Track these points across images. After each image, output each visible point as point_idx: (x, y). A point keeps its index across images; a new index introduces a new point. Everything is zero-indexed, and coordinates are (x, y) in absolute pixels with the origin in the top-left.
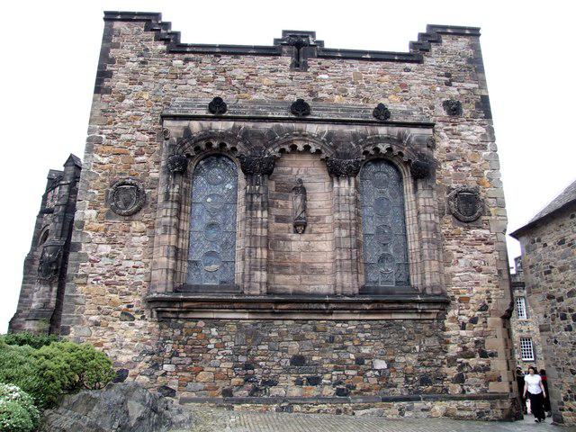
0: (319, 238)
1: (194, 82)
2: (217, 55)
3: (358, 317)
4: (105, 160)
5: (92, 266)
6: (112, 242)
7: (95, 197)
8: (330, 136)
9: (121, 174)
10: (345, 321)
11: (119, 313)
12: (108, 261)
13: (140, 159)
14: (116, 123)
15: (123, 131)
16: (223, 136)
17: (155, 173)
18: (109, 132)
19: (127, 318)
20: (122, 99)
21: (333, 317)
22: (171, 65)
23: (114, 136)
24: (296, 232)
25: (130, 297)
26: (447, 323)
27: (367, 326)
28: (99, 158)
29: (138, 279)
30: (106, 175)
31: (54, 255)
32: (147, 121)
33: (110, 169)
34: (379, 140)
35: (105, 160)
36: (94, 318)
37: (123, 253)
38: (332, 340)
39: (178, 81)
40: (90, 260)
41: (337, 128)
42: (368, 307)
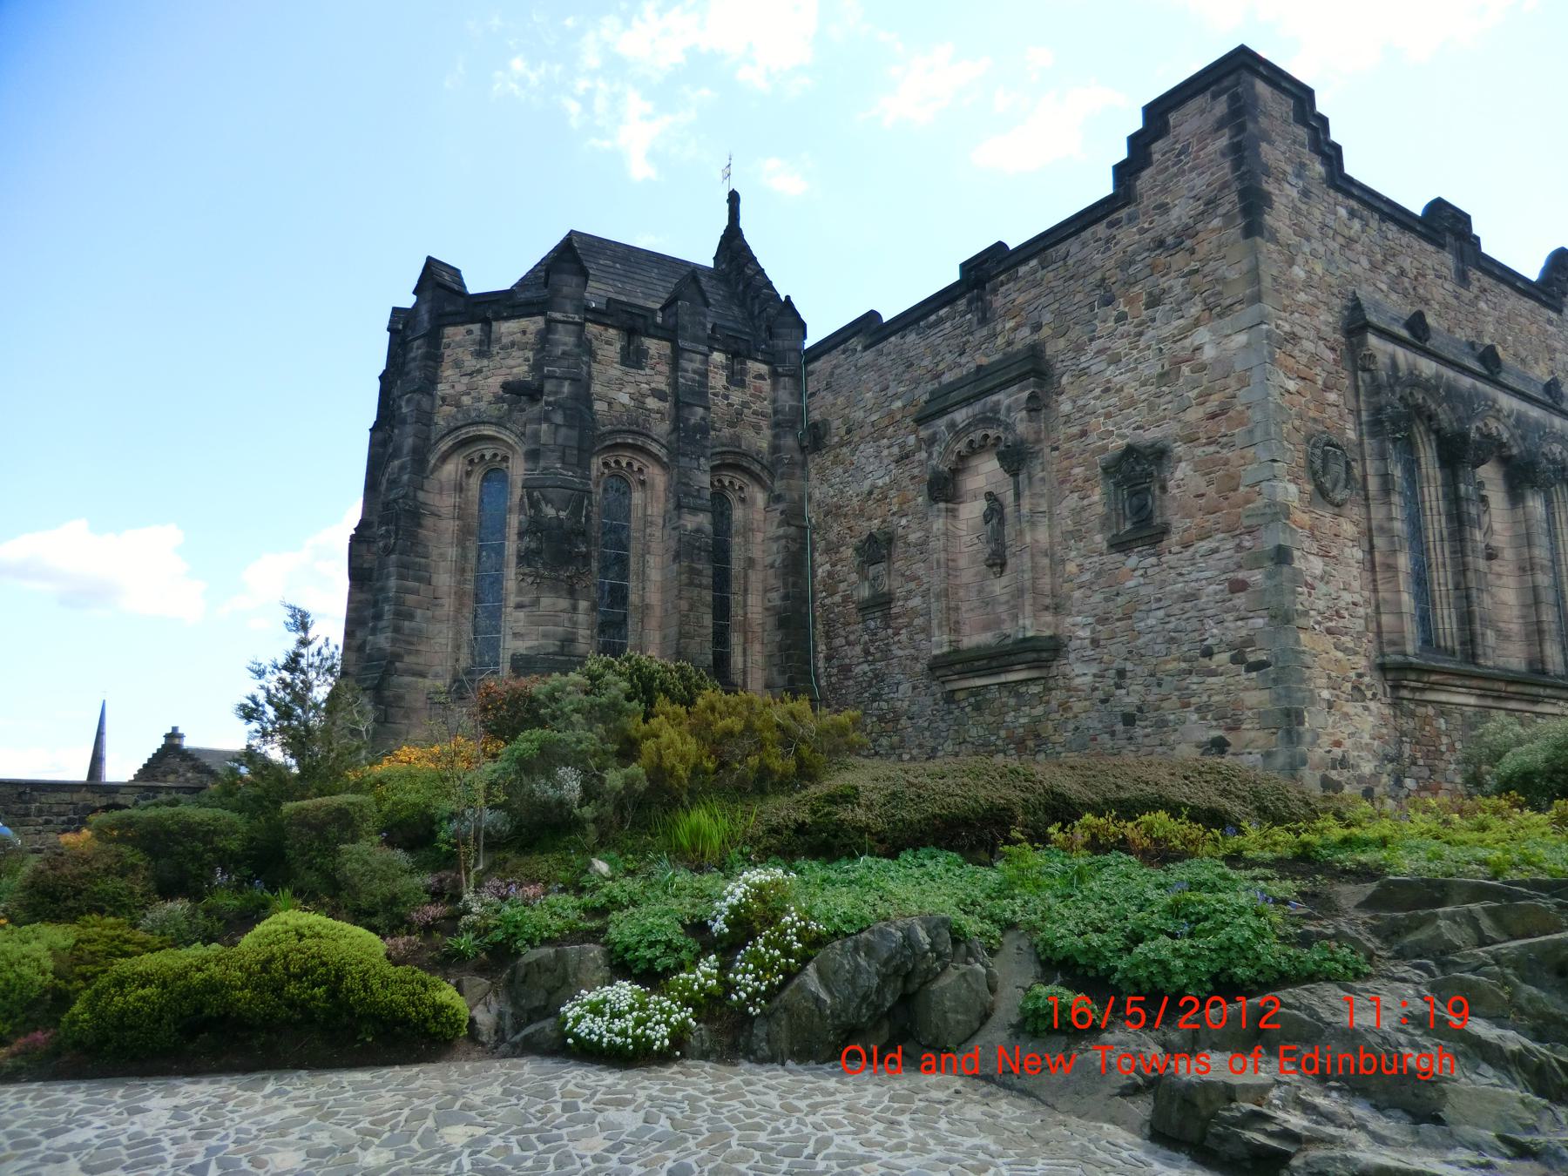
1: (1365, 262)
6: (1325, 554)
9: (1315, 420)
19: (1357, 695)
21: (1538, 708)
31: (576, 512)
32: (1327, 319)
36: (1326, 694)
39: (1348, 253)
40: (1307, 584)
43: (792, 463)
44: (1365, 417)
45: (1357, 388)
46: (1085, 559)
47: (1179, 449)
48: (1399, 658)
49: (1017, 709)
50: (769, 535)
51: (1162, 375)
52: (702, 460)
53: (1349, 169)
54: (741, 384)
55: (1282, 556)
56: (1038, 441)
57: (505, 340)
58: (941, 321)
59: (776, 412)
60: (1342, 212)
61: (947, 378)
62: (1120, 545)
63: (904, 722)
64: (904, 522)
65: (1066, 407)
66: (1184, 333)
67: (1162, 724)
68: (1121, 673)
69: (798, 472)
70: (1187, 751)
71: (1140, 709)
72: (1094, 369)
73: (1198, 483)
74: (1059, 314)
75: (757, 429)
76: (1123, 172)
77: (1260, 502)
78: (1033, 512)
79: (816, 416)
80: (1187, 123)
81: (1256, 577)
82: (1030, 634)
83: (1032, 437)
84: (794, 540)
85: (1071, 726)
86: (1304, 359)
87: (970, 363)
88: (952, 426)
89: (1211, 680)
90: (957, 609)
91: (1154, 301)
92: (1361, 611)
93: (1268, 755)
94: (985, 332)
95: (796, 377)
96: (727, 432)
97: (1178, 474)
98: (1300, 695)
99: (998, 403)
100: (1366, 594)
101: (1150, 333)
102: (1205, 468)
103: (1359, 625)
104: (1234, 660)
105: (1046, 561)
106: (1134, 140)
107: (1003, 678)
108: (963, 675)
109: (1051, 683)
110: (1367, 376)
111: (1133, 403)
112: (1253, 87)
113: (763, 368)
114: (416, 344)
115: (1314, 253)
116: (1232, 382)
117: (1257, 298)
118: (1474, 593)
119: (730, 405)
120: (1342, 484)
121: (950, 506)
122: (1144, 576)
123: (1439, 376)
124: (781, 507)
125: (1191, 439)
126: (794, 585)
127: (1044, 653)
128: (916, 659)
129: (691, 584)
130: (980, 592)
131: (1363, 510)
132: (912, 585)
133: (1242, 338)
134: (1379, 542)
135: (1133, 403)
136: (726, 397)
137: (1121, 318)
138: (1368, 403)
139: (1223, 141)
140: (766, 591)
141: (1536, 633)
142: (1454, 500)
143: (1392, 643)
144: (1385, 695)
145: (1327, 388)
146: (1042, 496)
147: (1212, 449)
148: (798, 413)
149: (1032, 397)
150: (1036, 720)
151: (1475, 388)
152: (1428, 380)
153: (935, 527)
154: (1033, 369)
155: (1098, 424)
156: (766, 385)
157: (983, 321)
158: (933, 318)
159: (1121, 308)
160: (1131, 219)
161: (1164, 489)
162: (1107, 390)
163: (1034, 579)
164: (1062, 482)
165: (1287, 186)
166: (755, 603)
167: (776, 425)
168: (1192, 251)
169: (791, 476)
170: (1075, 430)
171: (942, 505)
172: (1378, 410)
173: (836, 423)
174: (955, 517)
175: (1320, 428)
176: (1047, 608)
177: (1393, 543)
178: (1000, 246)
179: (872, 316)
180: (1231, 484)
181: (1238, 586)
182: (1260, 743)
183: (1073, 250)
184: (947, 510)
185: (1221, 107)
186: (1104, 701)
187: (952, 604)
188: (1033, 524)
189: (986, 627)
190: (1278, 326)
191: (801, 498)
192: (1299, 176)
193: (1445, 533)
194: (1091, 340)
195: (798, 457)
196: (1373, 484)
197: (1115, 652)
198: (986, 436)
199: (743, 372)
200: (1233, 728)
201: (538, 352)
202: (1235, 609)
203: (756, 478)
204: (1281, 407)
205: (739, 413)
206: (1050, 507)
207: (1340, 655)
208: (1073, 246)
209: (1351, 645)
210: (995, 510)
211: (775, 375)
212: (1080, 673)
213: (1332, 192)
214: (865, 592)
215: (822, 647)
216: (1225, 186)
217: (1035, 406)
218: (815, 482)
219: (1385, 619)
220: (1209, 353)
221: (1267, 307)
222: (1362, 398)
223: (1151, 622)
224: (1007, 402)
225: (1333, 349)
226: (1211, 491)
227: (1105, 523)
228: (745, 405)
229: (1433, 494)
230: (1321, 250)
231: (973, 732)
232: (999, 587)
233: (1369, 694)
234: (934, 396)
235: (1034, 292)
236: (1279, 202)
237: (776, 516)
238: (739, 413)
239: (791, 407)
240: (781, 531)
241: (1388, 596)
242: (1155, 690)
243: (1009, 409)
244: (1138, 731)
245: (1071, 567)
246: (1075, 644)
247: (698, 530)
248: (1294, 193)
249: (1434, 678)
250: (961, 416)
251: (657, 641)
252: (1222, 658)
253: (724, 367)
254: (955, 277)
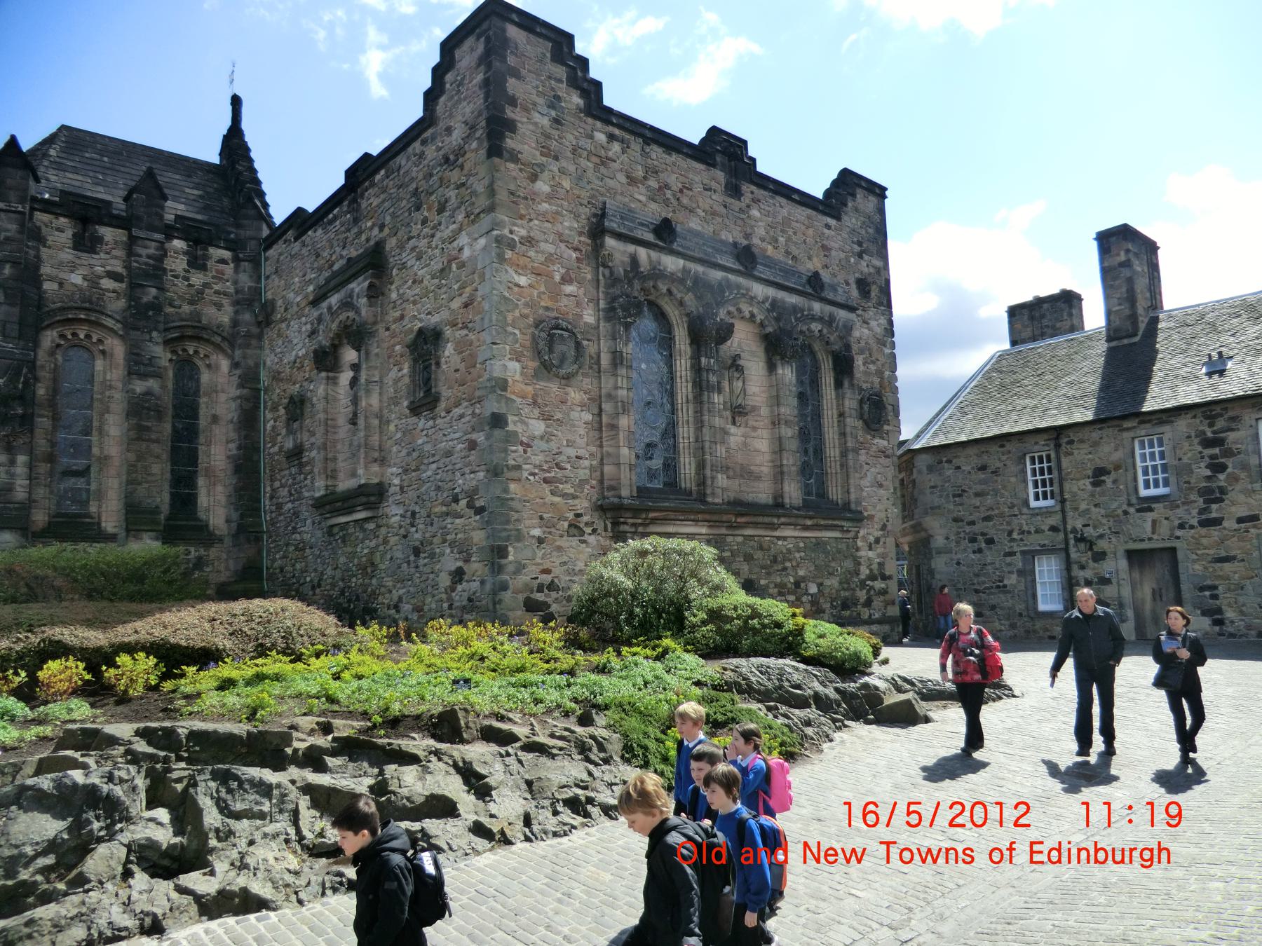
0: (753, 434)
1: (622, 178)
2: (647, 141)
3: (796, 534)
4: (523, 281)
5: (525, 452)
6: (547, 418)
7: (517, 342)
8: (775, 304)
9: (547, 309)
10: (785, 538)
11: (566, 524)
12: (544, 445)
13: (569, 289)
14: (531, 220)
15: (542, 237)
16: (672, 278)
17: (589, 317)
18: (523, 232)
19: (575, 531)
20: (534, 178)
21: (777, 533)
22: (592, 137)
23: (529, 241)
24: (734, 423)
25: (577, 502)
26: (860, 543)
27: (802, 545)
28: (516, 277)
29: (583, 474)
30: (526, 305)
32: (570, 225)
33: (531, 295)
34: (813, 318)
35: (523, 281)
36: (537, 532)
37: (562, 435)
38: (775, 561)
39: (603, 170)
40: (522, 443)
41: (781, 295)
42: (809, 522)
43: (249, 335)
44: (602, 304)
45: (598, 281)
46: (398, 421)
47: (448, 332)
48: (616, 500)
50: (231, 395)
51: (443, 270)
52: (155, 334)
53: (608, 101)
54: (203, 268)
55: (498, 421)
56: (375, 323)
58: (335, 218)
59: (237, 292)
60: (601, 137)
61: (336, 267)
62: (415, 410)
65: (394, 296)
67: (432, 556)
69: (254, 342)
74: (394, 216)
75: (219, 306)
76: (430, 97)
77: (486, 376)
78: (368, 382)
79: (269, 295)
82: (363, 482)
83: (371, 320)
84: (247, 400)
86: (541, 258)
89: (458, 521)
90: (335, 459)
92: (586, 463)
93: (483, 582)
95: (256, 263)
96: (186, 309)
97: (447, 353)
98: (504, 534)
99: (352, 290)
100: (593, 449)
101: (438, 235)
102: (461, 347)
103: (583, 474)
105: (376, 422)
109: (380, 522)
110: (607, 272)
112: (504, 31)
113: (227, 254)
115: (562, 171)
116: (476, 276)
117: (491, 209)
118: (707, 445)
119: (190, 285)
120: (571, 359)
121: (331, 374)
122: (426, 435)
123: (685, 271)
124: (238, 372)
125: (454, 325)
126: (246, 437)
129: (139, 439)
131: (595, 382)
133: (482, 241)
134: (607, 407)
136: (187, 279)
138: (606, 294)
139: (480, 77)
140: (228, 442)
141: (779, 474)
142: (697, 369)
143: (612, 488)
144: (606, 530)
145: (566, 280)
146: (376, 368)
147: (465, 332)
148: (257, 292)
149: (371, 286)
151: (728, 280)
152: (672, 274)
154: (375, 263)
155: (411, 310)
156: (229, 269)
159: (426, 214)
161: (438, 364)
162: (414, 282)
163: (367, 437)
165: (537, 115)
166: (217, 451)
167: (236, 303)
168: (462, 167)
169: (248, 346)
171: (324, 374)
172: (614, 299)
173: (280, 303)
174: (336, 384)
175: (554, 314)
176: (376, 461)
177: (616, 407)
178: (366, 156)
179: (300, 211)
182: (479, 573)
183: (403, 163)
184: (328, 378)
186: (405, 537)
187: (330, 455)
188: (368, 391)
190: (511, 232)
191: (257, 365)
192: (551, 106)
193: (691, 397)
194: (410, 238)
195: (255, 330)
196: (605, 360)
199: (206, 257)
202: (469, 464)
203: (218, 347)
204: (505, 298)
205: (200, 292)
206: (381, 378)
207: (557, 499)
208: (401, 160)
209: (572, 491)
211: (237, 260)
212: (393, 512)
213: (590, 120)
214: (289, 444)
215: (268, 489)
217: (375, 293)
218: (267, 351)
219: (607, 469)
221: (501, 216)
222: (601, 289)
223: (429, 473)
224: (357, 290)
225: (576, 249)
226: (462, 367)
228: (206, 285)
229: (683, 365)
230: (572, 168)
233: (588, 530)
235: (382, 196)
236: (524, 128)
237: (235, 380)
238: (200, 292)
239: (250, 288)
240: (238, 392)
241: (610, 450)
242: (430, 528)
244: (421, 562)
245: (392, 428)
246: (392, 490)
247: (148, 393)
248: (545, 121)
249: (652, 515)
251: (116, 485)
253: (185, 253)
254: (341, 181)
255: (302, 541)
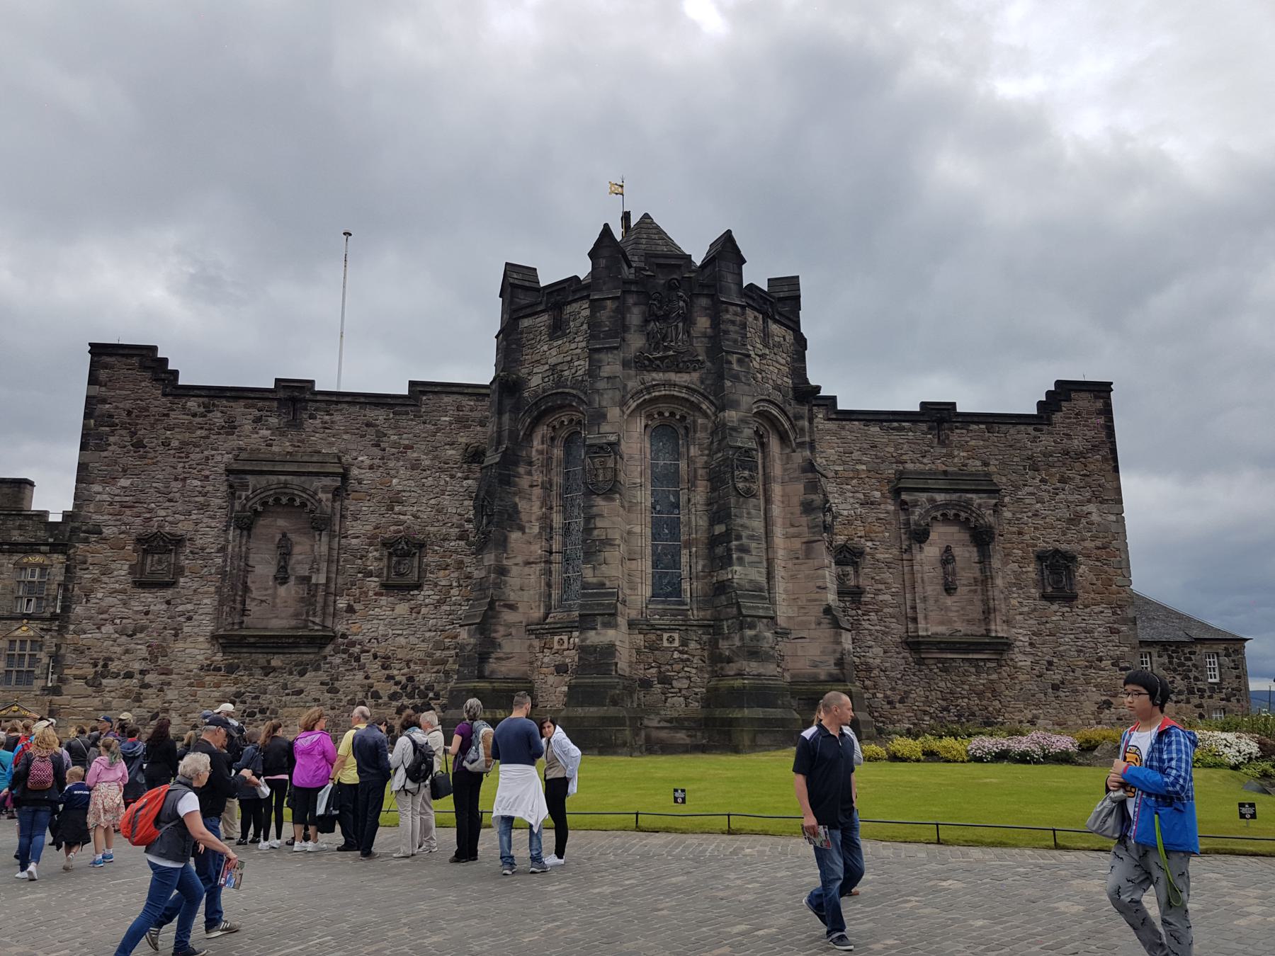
47: (1080, 558)
49: (978, 673)
51: (1070, 521)
57: (777, 339)
58: (901, 429)
61: (910, 466)
63: (876, 672)
64: (869, 544)
65: (1008, 515)
66: (1082, 503)
68: (1050, 663)
70: (1089, 707)
71: (1063, 683)
72: (1027, 501)
73: (1091, 577)
80: (1083, 402)
81: (1124, 628)
85: (1018, 687)
87: (927, 465)
88: (932, 501)
91: (1063, 480)
94: (944, 451)
104: (1113, 665)
106: (1048, 393)
107: (970, 656)
108: (942, 650)
111: (1053, 528)
114: (732, 309)
127: (1002, 647)
128: (885, 633)
130: (936, 601)
132: (883, 587)
135: (1053, 528)
137: (1042, 481)
139: (1102, 421)
149: (996, 505)
150: (992, 682)
153: (918, 557)
157: (942, 443)
158: (895, 424)
160: (1050, 433)
164: (1008, 555)
170: (1015, 529)
180: (1108, 583)
181: (1113, 631)
185: (1099, 404)
189: (942, 623)
197: (1046, 651)
198: (957, 515)
200: (1115, 696)
201: (794, 360)
210: (947, 558)
216: (1103, 442)
217: (996, 509)
220: (1095, 517)
227: (1040, 583)
231: (942, 684)
232: (949, 601)
234: (901, 475)
243: (980, 505)
250: (940, 497)
252: (1107, 663)
255: (867, 664)
